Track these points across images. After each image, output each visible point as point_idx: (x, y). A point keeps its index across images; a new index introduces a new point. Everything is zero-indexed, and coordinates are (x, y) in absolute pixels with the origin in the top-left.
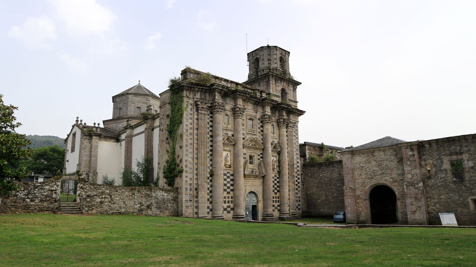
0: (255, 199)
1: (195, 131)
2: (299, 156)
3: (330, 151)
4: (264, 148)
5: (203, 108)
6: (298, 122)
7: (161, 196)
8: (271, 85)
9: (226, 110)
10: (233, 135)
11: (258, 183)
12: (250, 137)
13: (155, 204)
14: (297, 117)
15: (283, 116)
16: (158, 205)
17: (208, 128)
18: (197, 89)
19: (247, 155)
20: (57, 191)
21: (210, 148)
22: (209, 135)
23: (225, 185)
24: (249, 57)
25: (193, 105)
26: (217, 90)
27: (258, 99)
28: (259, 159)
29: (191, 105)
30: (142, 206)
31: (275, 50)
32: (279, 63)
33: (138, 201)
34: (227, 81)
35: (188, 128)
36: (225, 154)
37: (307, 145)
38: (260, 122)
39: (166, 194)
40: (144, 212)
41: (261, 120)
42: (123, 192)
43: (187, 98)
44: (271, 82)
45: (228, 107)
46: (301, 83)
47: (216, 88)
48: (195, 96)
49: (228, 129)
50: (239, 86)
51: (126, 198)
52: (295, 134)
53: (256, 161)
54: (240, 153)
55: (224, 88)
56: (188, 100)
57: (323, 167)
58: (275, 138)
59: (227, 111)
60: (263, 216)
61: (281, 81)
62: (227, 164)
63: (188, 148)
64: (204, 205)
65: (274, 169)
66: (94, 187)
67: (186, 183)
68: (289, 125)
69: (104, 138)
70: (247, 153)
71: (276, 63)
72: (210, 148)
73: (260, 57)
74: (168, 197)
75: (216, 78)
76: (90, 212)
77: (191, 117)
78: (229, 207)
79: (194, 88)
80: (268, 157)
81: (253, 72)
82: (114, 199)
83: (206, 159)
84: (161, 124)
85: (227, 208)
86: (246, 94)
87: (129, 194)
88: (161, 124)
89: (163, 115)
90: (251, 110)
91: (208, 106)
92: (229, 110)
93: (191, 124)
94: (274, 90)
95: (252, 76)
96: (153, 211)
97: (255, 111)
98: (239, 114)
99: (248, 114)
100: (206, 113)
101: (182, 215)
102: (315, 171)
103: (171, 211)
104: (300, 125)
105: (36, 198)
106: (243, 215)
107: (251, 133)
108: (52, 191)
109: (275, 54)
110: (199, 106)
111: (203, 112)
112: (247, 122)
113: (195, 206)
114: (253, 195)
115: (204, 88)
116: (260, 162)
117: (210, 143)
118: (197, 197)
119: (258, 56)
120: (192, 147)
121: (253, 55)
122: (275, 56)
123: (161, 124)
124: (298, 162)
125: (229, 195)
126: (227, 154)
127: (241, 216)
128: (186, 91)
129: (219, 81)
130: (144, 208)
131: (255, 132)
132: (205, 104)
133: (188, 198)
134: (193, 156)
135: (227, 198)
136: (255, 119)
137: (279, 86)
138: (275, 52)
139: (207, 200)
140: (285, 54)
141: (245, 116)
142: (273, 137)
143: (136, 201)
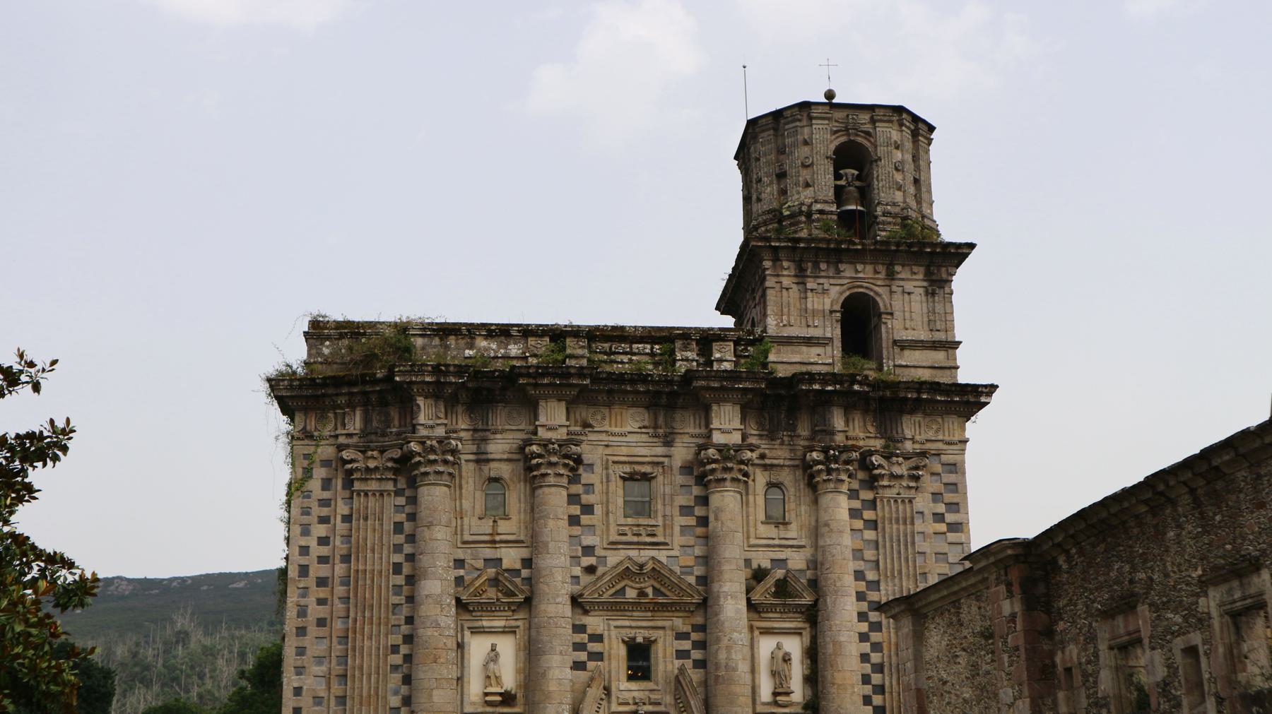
1: (340, 569)
5: (368, 469)
6: (965, 441)
9: (488, 461)
10: (527, 563)
14: (951, 422)
15: (832, 433)
17: (398, 548)
18: (342, 400)
19: (606, 640)
21: (405, 629)
22: (402, 577)
25: (334, 466)
27: (658, 383)
28: (682, 654)
29: (326, 463)
31: (805, 122)
34: (502, 332)
35: (311, 560)
36: (478, 648)
38: (690, 480)
41: (695, 474)
43: (306, 442)
44: (770, 282)
46: (971, 246)
47: (411, 382)
48: (344, 425)
49: (498, 538)
50: (569, 341)
52: (941, 508)
53: (665, 662)
54: (545, 638)
55: (446, 374)
56: (312, 449)
58: (790, 542)
59: (493, 465)
62: (490, 690)
63: (307, 641)
70: (609, 630)
71: (807, 185)
72: (405, 629)
75: (445, 331)
77: (325, 511)
79: (330, 396)
83: (385, 676)
86: (569, 375)
90: (630, 438)
91: (392, 459)
92: (505, 457)
93: (323, 541)
99: (611, 458)
100: (390, 486)
104: (973, 459)
107: (635, 539)
109: (806, 143)
111: (373, 486)
112: (607, 493)
115: (368, 388)
116: (682, 670)
117: (405, 611)
120: (327, 634)
122: (807, 149)
126: (493, 648)
128: (306, 415)
129: (462, 342)
131: (659, 531)
132: (382, 452)
134: (330, 669)
140: (873, 121)
142: (777, 542)
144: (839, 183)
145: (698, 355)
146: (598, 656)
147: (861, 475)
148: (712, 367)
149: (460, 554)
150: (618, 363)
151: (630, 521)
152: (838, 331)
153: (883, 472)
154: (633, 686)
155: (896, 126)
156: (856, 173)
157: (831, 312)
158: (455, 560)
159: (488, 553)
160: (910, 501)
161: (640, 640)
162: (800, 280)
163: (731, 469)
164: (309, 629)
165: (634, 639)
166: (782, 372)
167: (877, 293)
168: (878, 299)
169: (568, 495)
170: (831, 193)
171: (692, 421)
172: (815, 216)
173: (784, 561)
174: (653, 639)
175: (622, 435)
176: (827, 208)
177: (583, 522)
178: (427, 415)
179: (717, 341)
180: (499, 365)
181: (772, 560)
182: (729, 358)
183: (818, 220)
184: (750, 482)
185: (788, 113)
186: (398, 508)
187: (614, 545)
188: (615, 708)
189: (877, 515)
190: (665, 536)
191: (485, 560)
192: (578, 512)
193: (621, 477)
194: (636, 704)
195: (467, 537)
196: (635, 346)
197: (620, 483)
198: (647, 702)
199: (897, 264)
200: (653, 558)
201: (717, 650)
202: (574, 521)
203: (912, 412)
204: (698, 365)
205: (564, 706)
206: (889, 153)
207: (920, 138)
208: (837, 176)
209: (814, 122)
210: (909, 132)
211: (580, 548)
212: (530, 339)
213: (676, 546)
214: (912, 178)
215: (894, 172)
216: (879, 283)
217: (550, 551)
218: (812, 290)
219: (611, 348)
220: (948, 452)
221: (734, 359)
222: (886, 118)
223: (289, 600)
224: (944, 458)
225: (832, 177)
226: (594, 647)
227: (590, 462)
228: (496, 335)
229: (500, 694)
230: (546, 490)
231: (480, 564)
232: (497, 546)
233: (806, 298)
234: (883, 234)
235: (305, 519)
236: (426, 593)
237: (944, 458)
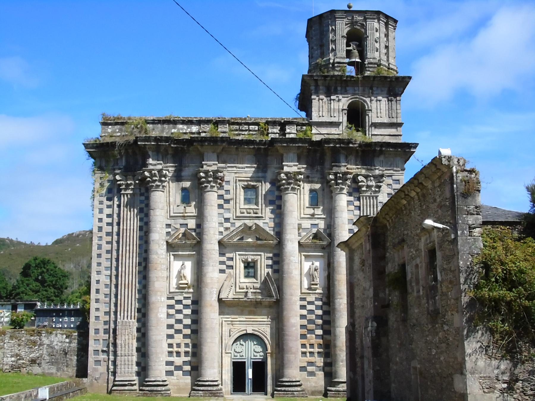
0: (259, 349)
7: (60, 344)
13: (47, 358)
16: (53, 359)
26: (147, 147)
30: (19, 359)
33: (11, 352)
34: (190, 122)
38: (274, 188)
40: (24, 370)
46: (410, 78)
48: (117, 164)
49: (186, 215)
62: (181, 282)
64: (128, 359)
65: (313, 284)
67: (96, 320)
78: (185, 363)
85: (184, 365)
93: (108, 216)
96: (44, 369)
99: (237, 178)
106: (217, 381)
107: (248, 215)
113: (112, 361)
118: (115, 345)
120: (110, 257)
130: (23, 363)
135: (183, 345)
141: (232, 183)
143: (5, 351)
144: (348, 48)
145: (279, 130)
146: (231, 267)
147: (354, 185)
148: (285, 136)
149: (169, 222)
150: (243, 135)
151: (247, 207)
152: (345, 118)
153: (364, 184)
154: (247, 280)
155: (376, 21)
156: (358, 43)
157: (343, 110)
158: (166, 225)
159: (182, 221)
160: (377, 197)
161: (250, 260)
163: (291, 183)
164: (102, 255)
165: (247, 259)
166: (316, 138)
169: (218, 195)
170: (344, 54)
171: (275, 161)
172: (336, 65)
173: (317, 225)
175: (243, 168)
176: (342, 61)
177: (224, 207)
180: (187, 137)
181: (311, 224)
182: (293, 132)
183: (338, 67)
184: (301, 188)
185: (325, 15)
186: (141, 202)
187: (238, 218)
188: (238, 290)
189: (360, 203)
190: (262, 214)
191: (181, 225)
192: (223, 203)
193: (242, 187)
194: (247, 288)
195: (172, 214)
196: (250, 127)
197: (242, 190)
198: (252, 287)
199: (375, 87)
200: (255, 224)
202: (220, 206)
203: (378, 156)
204: (279, 136)
205: (213, 289)
206: (373, 34)
207: (390, 26)
208: (348, 45)
209: (337, 20)
210: (384, 23)
211: (223, 219)
213: (267, 218)
214: (384, 46)
215: (375, 43)
217: (208, 220)
219: (239, 128)
220: (395, 174)
221: (296, 132)
222: (371, 17)
223: (93, 242)
224: (394, 177)
225: (345, 46)
226: (229, 263)
227: (228, 180)
229: (187, 284)
230: (208, 193)
231: (178, 226)
233: (331, 103)
234: (369, 72)
235: (101, 206)
237: (394, 177)
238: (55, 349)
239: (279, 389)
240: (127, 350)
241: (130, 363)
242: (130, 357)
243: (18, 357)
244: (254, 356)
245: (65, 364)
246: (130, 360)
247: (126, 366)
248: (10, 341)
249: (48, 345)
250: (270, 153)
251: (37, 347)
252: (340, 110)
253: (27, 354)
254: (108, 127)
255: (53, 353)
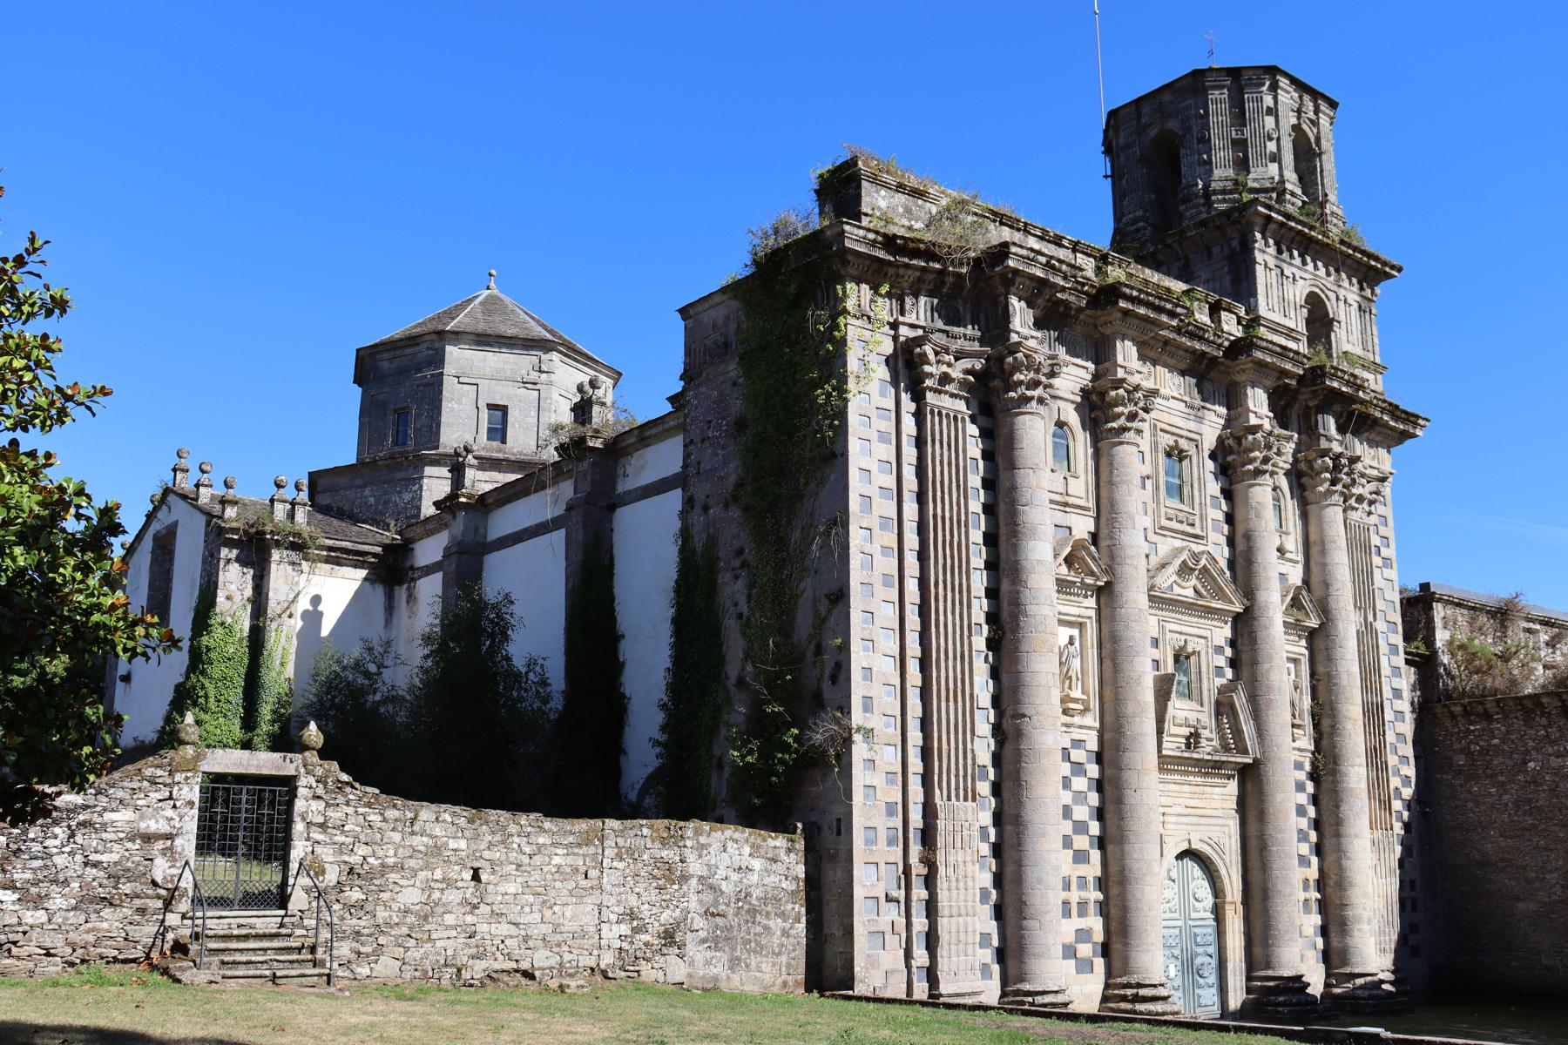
2: (1400, 660)
3: (1544, 637)
4: (1247, 610)
7: (735, 877)
8: (1259, 270)
11: (1219, 804)
12: (1179, 551)
13: (699, 923)
15: (1329, 439)
20: (178, 842)
23: (1067, 812)
24: (1116, 132)
26: (1018, 279)
30: (636, 930)
32: (1288, 158)
37: (1439, 600)
39: (757, 864)
42: (540, 847)
43: (859, 323)
44: (1259, 257)
45: (1074, 376)
48: (902, 313)
49: (1071, 500)
51: (558, 884)
57: (1544, 721)
59: (1060, 403)
60: (1249, 991)
61: (1302, 255)
66: (385, 820)
67: (866, 796)
68: (1354, 491)
69: (328, 560)
70: (1164, 634)
73: (1188, 130)
74: (767, 880)
76: (363, 971)
78: (1083, 935)
80: (1270, 658)
81: (1146, 210)
82: (490, 888)
84: (698, 473)
87: (570, 860)
88: (692, 470)
89: (709, 422)
94: (1276, 299)
95: (1138, 230)
96: (692, 963)
97: (1192, 407)
98: (1122, 421)
101: (849, 982)
102: (1496, 741)
103: (784, 959)
105: (55, 881)
108: (148, 838)
109: (1270, 111)
110: (927, 368)
111: (946, 402)
114: (1197, 871)
119: (1172, 125)
121: (1139, 116)
122: (1270, 121)
123: (698, 473)
124: (1397, 693)
125: (1083, 870)
127: (1155, 986)
128: (858, 284)
130: (646, 944)
133: (882, 884)
136: (1193, 451)
137: (1294, 279)
138: (1268, 101)
139: (978, 898)
140: (1317, 111)
162: (1279, 263)
167: (1326, 296)
168: (1327, 303)
174: (1197, 650)
178: (1021, 317)
179: (1225, 310)
201: (1268, 671)
212: (1078, 255)
213: (1210, 543)
216: (1329, 286)
218: (1287, 277)
228: (1049, 241)
232: (1068, 509)
236: (1037, 557)
238: (722, 892)
239: (1282, 999)
240: (962, 897)
241: (970, 941)
242: (969, 919)
243: (635, 923)
244: (1196, 911)
245: (753, 945)
246: (970, 929)
247: (962, 947)
248: (615, 864)
249: (701, 878)
250: (1212, 374)
251: (676, 887)
252: (1298, 307)
253: (655, 910)
254: (878, 192)
255: (716, 907)
